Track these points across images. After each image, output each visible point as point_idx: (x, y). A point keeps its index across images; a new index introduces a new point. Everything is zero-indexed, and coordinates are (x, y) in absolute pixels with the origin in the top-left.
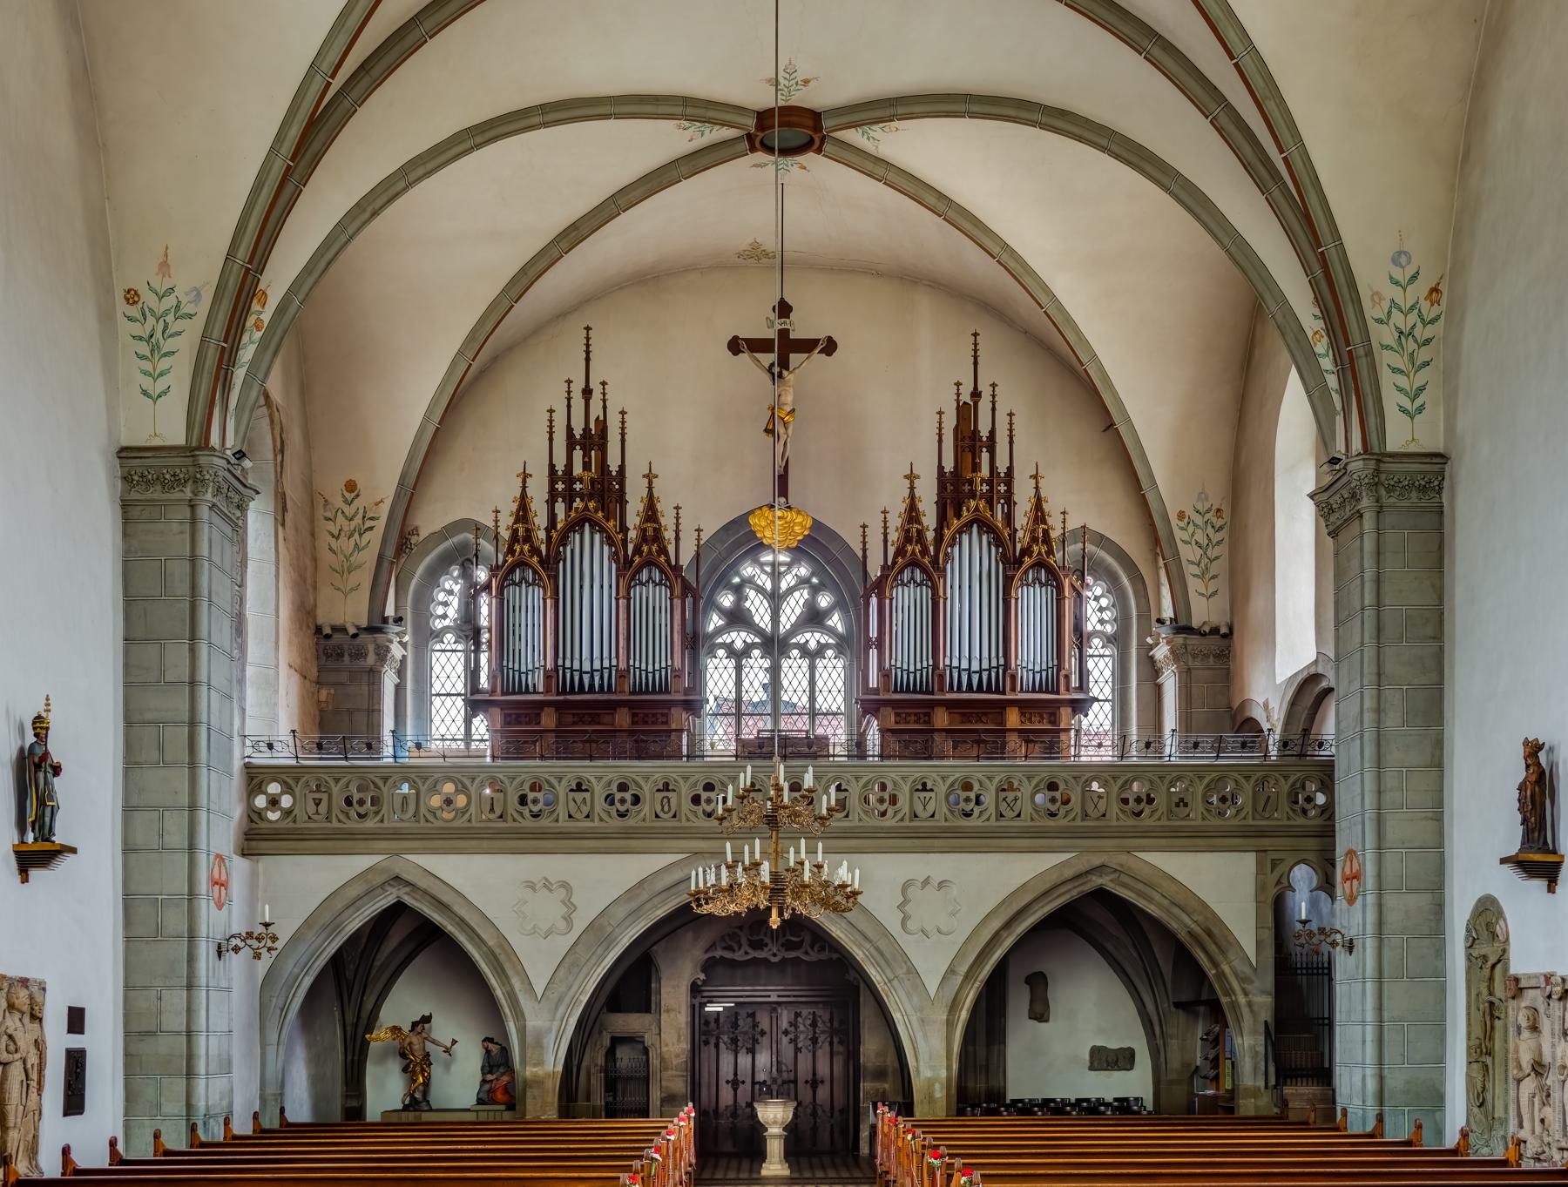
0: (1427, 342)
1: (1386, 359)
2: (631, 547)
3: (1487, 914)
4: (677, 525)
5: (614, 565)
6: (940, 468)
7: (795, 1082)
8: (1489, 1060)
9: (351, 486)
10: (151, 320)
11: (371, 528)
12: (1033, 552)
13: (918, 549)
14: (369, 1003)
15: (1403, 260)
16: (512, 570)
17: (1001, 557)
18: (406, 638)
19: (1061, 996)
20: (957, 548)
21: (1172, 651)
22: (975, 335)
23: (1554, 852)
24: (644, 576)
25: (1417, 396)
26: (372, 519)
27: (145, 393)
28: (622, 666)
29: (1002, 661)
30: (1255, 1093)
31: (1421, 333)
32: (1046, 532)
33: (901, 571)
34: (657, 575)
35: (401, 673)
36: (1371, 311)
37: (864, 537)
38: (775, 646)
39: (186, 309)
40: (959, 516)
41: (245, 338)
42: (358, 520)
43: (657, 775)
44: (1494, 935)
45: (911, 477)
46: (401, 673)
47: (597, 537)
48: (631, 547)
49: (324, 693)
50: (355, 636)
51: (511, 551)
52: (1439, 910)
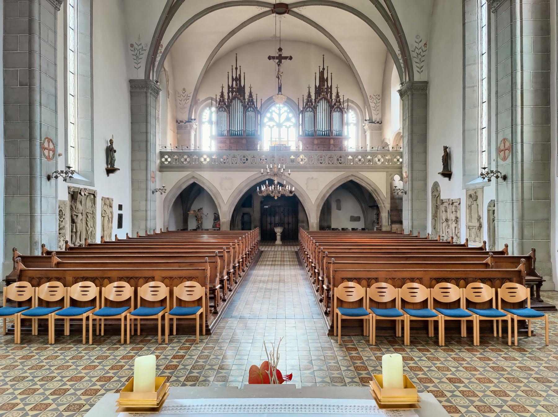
0: (424, 56)
1: (414, 60)
2: (246, 103)
3: (436, 186)
4: (257, 98)
6: (316, 86)
7: (284, 223)
8: (436, 218)
9: (184, 89)
10: (136, 51)
11: (189, 99)
13: (310, 104)
14: (189, 205)
15: (418, 37)
16: (220, 108)
18: (197, 124)
19: (344, 205)
21: (368, 127)
22: (323, 55)
23: (450, 171)
24: (249, 109)
25: (421, 68)
26: (189, 97)
27: (135, 68)
28: (244, 130)
29: (329, 129)
30: (386, 226)
31: (422, 54)
32: (339, 100)
34: (252, 109)
35: (196, 131)
36: (411, 49)
38: (279, 125)
39: (144, 48)
40: (320, 96)
41: (158, 55)
42: (186, 97)
44: (437, 190)
45: (309, 88)
46: (196, 131)
47: (239, 101)
48: (246, 103)
49: (178, 135)
50: (185, 123)
51: (219, 104)
52: (426, 185)
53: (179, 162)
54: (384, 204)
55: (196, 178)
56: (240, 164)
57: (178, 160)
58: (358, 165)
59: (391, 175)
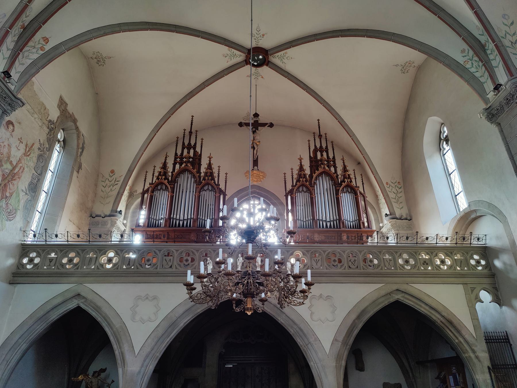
4: (219, 172)
5: (195, 185)
12: (345, 181)
13: (304, 180)
16: (157, 185)
17: (334, 184)
20: (318, 181)
29: (338, 218)
33: (299, 188)
37: (285, 177)
43: (202, 250)
47: (190, 175)
51: (158, 178)
53: (54, 265)
54: (474, 352)
55: (84, 298)
56: (178, 267)
57: (54, 261)
58: (405, 271)
59: (472, 291)
